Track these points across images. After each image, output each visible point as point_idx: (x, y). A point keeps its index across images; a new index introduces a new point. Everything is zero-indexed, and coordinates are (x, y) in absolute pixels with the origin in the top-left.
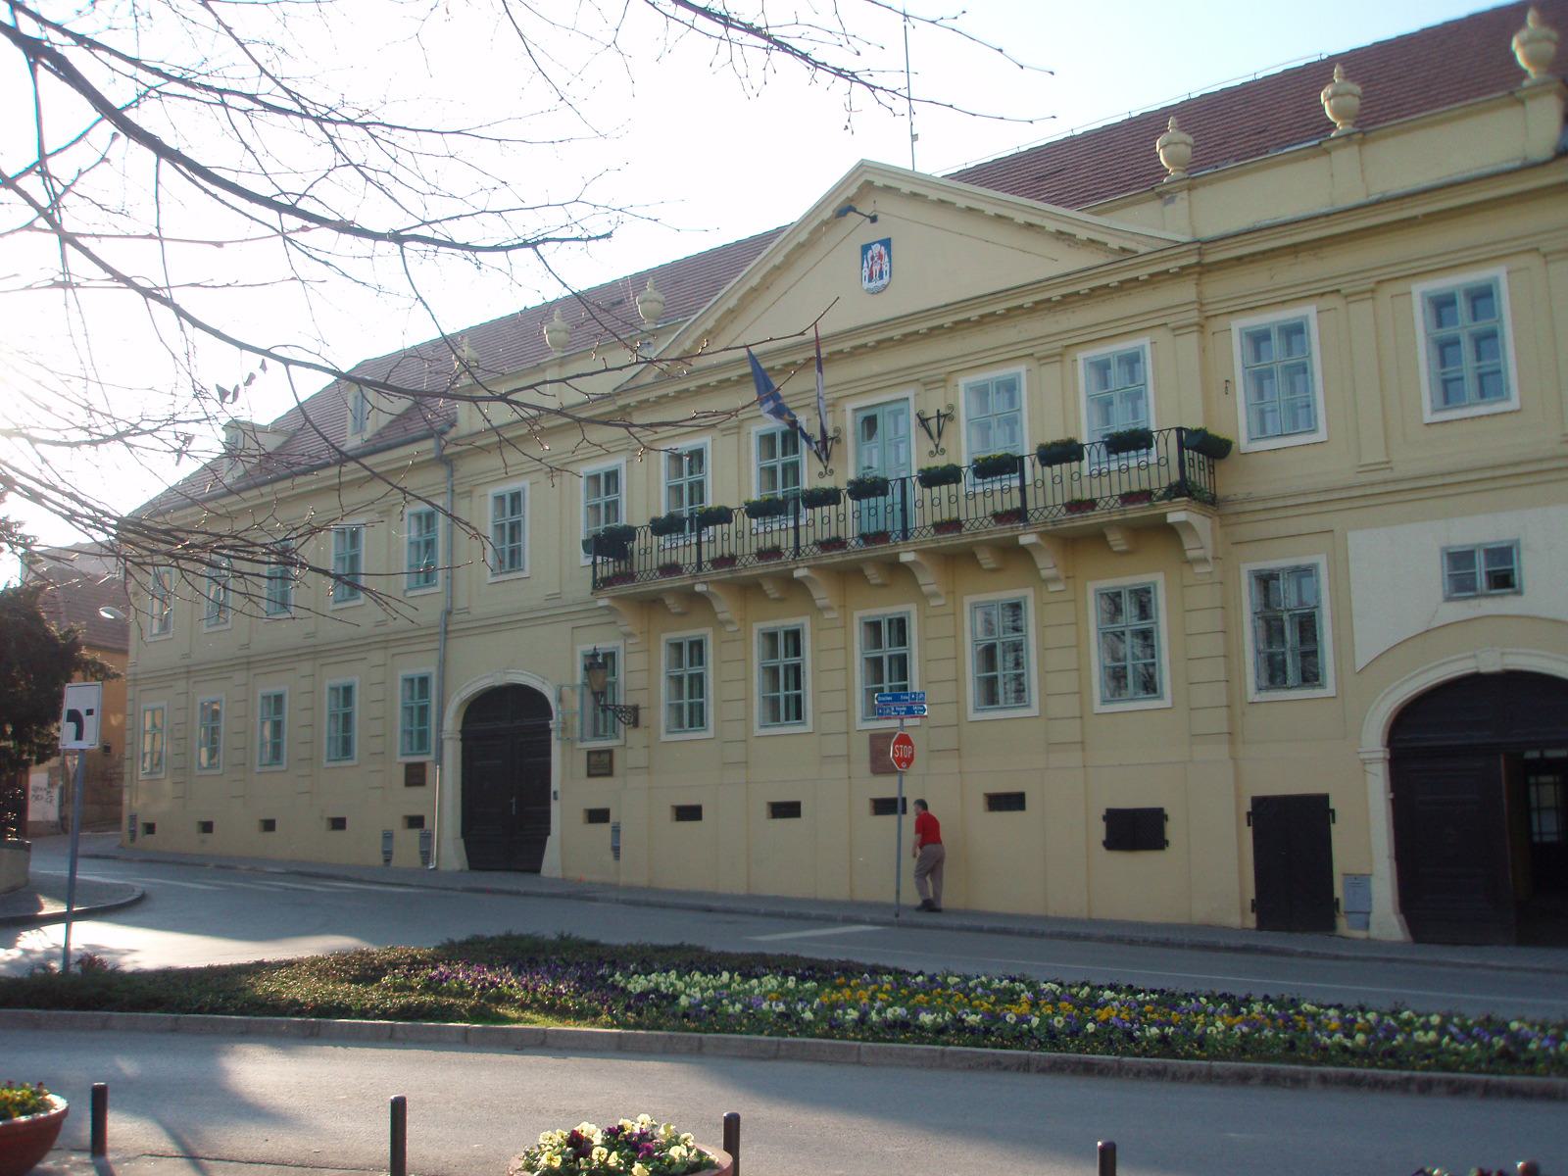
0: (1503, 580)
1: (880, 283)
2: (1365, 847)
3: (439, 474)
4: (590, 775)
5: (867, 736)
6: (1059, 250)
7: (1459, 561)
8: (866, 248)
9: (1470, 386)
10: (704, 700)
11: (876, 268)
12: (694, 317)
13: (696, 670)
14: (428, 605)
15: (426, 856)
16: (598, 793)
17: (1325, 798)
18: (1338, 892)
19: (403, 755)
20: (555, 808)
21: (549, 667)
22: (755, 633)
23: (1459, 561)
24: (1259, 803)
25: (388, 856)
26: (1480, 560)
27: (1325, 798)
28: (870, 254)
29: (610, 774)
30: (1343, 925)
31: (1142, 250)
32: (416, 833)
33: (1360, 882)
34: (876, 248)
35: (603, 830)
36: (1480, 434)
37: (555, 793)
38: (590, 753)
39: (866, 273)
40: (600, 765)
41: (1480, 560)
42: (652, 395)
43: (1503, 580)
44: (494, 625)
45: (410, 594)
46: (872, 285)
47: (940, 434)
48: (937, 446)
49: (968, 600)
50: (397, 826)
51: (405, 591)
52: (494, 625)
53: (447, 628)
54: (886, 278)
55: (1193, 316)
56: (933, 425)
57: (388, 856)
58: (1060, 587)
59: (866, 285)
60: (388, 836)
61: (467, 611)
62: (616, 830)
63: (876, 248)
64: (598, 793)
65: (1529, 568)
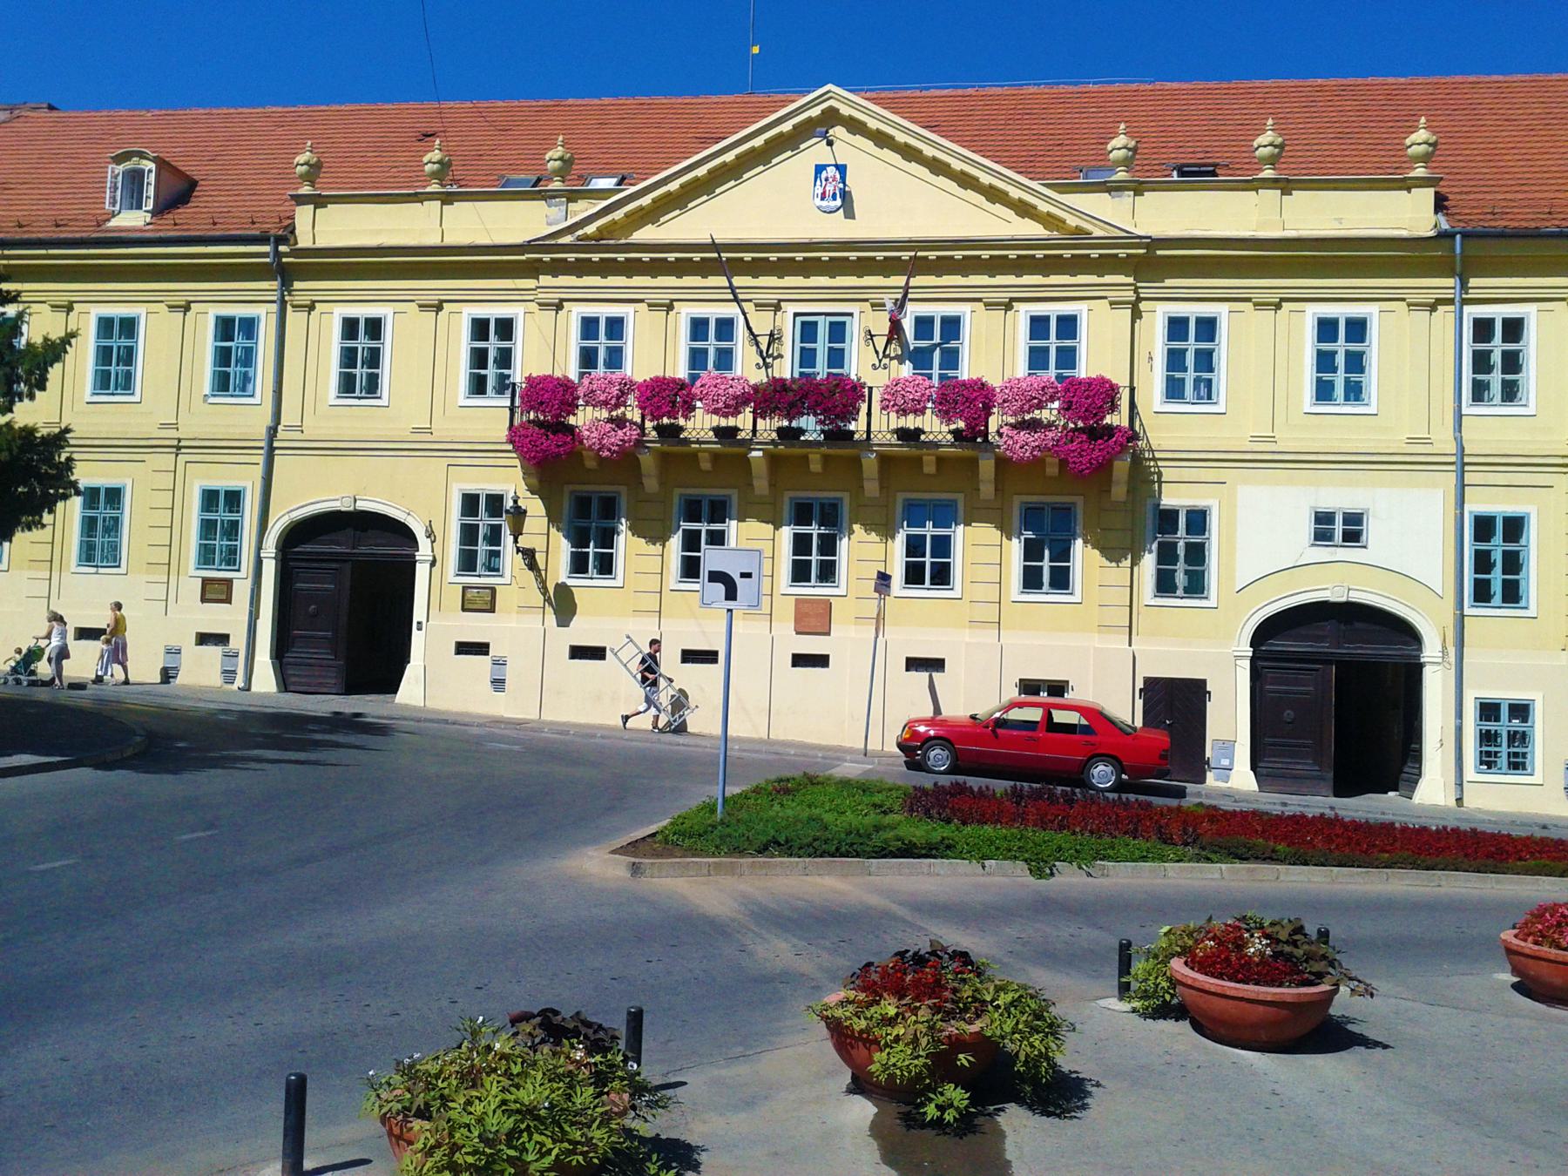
0: (1353, 536)
2: (1230, 720)
4: (464, 609)
7: (1323, 519)
8: (820, 169)
9: (1339, 390)
11: (830, 188)
15: (229, 675)
16: (475, 627)
17: (1204, 682)
18: (1208, 754)
20: (417, 638)
21: (426, 504)
22: (676, 500)
23: (1323, 519)
24: (1147, 681)
26: (1339, 519)
27: (1204, 682)
28: (824, 175)
30: (1211, 779)
31: (1097, 233)
32: (214, 652)
33: (1228, 747)
36: (1340, 428)
39: (819, 191)
41: (1339, 519)
43: (1353, 536)
46: (824, 203)
55: (1129, 295)
57: (167, 675)
59: (818, 201)
62: (499, 663)
63: (831, 171)
64: (475, 627)
65: (1373, 530)
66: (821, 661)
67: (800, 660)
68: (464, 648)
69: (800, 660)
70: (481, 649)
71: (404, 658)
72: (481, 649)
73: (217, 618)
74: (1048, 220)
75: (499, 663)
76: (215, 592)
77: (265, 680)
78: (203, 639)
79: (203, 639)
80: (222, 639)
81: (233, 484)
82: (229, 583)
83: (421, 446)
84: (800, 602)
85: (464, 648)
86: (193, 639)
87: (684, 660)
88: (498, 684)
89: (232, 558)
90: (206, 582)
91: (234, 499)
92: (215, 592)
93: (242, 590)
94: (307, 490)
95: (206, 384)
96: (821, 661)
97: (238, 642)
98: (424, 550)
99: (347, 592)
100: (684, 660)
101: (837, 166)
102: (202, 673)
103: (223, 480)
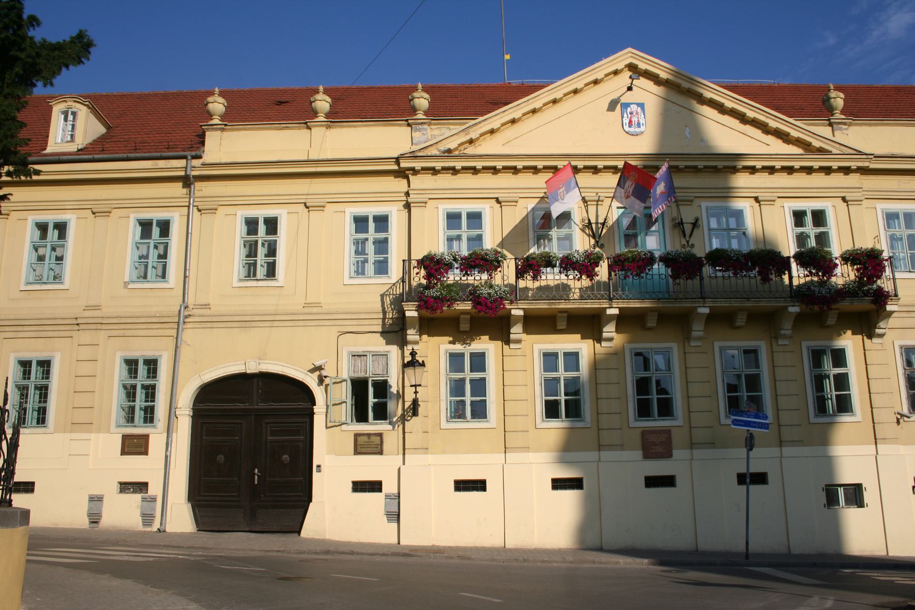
1: (638, 130)
3: (177, 189)
4: (357, 452)
5: (639, 431)
6: (770, 139)
10: (544, 398)
11: (635, 119)
12: (481, 119)
13: (477, 375)
14: (162, 297)
15: (147, 518)
16: (368, 467)
19: (118, 426)
25: (95, 519)
28: (629, 110)
29: (381, 453)
31: (835, 151)
32: (136, 498)
34: (634, 108)
37: (319, 466)
38: (357, 436)
39: (626, 121)
40: (368, 446)
42: (438, 165)
44: (245, 322)
47: (691, 236)
48: (688, 242)
49: (717, 345)
50: (110, 491)
51: (126, 284)
52: (245, 322)
53: (182, 318)
54: (642, 128)
56: (688, 228)
57: (95, 519)
58: (786, 342)
59: (626, 128)
60: (96, 500)
61: (207, 306)
63: (634, 108)
64: (368, 467)
66: (668, 481)
67: (652, 482)
68: (360, 487)
69: (652, 482)
70: (374, 486)
72: (374, 486)
73: (136, 468)
74: (798, 142)
76: (135, 446)
77: (180, 518)
78: (125, 487)
79: (125, 487)
80: (142, 487)
81: (150, 354)
82: (146, 438)
83: (311, 316)
84: (645, 433)
85: (360, 487)
86: (116, 487)
87: (555, 487)
88: (395, 516)
89: (149, 415)
90: (125, 438)
91: (152, 365)
92: (135, 446)
93: (157, 442)
95: (128, 270)
96: (668, 481)
97: (155, 489)
99: (252, 443)
100: (555, 487)
101: (638, 105)
102: (123, 513)
103: (141, 350)
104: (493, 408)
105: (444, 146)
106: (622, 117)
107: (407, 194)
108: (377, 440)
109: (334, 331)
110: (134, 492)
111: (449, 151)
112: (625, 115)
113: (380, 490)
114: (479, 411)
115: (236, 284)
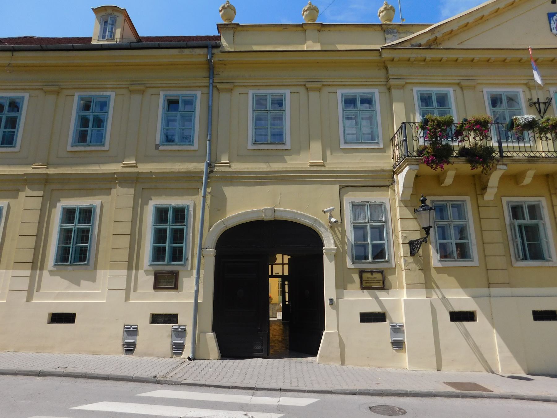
20: (329, 313)
35: (383, 328)
45: (161, 148)
51: (157, 147)
68: (366, 317)
70: (380, 317)
71: (322, 327)
72: (380, 317)
73: (166, 301)
75: (397, 330)
76: (166, 281)
78: (156, 319)
79: (156, 319)
80: (171, 319)
85: (366, 317)
86: (148, 319)
88: (398, 345)
89: (177, 255)
92: (166, 281)
94: (246, 204)
97: (186, 320)
98: (329, 244)
104: (474, 250)
105: (413, 42)
106: (550, 23)
107: (388, 79)
108: (379, 276)
109: (336, 187)
110: (165, 322)
111: (420, 45)
112: (552, 22)
113: (384, 320)
114: (463, 252)
115: (250, 147)
